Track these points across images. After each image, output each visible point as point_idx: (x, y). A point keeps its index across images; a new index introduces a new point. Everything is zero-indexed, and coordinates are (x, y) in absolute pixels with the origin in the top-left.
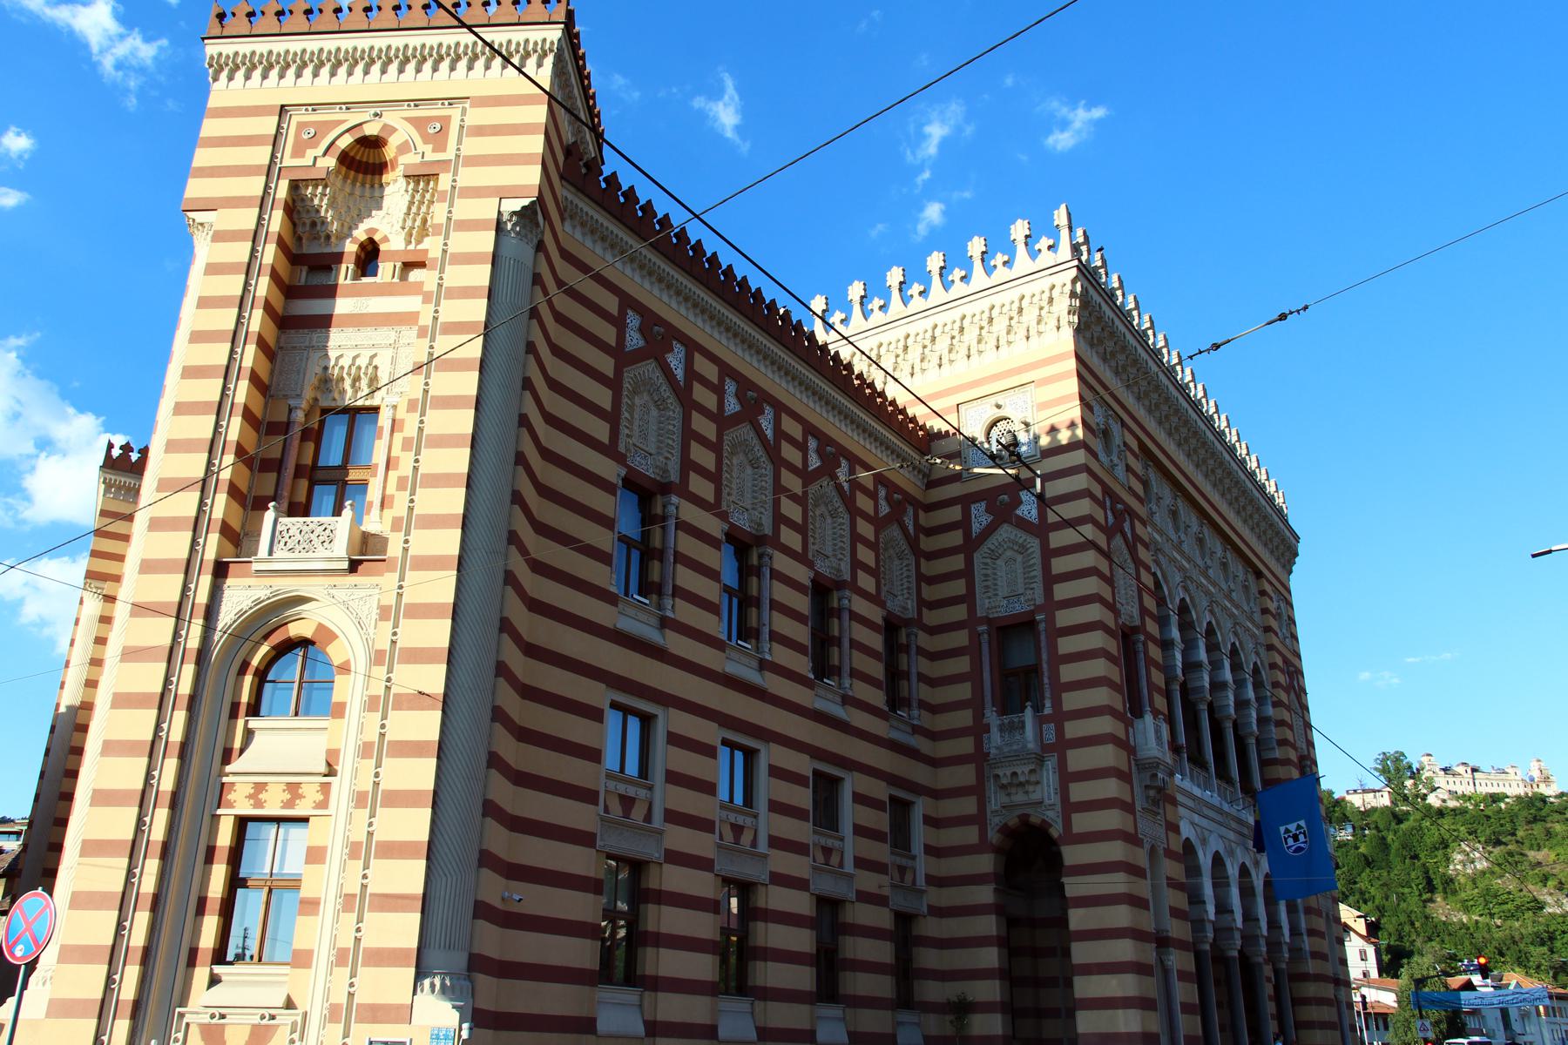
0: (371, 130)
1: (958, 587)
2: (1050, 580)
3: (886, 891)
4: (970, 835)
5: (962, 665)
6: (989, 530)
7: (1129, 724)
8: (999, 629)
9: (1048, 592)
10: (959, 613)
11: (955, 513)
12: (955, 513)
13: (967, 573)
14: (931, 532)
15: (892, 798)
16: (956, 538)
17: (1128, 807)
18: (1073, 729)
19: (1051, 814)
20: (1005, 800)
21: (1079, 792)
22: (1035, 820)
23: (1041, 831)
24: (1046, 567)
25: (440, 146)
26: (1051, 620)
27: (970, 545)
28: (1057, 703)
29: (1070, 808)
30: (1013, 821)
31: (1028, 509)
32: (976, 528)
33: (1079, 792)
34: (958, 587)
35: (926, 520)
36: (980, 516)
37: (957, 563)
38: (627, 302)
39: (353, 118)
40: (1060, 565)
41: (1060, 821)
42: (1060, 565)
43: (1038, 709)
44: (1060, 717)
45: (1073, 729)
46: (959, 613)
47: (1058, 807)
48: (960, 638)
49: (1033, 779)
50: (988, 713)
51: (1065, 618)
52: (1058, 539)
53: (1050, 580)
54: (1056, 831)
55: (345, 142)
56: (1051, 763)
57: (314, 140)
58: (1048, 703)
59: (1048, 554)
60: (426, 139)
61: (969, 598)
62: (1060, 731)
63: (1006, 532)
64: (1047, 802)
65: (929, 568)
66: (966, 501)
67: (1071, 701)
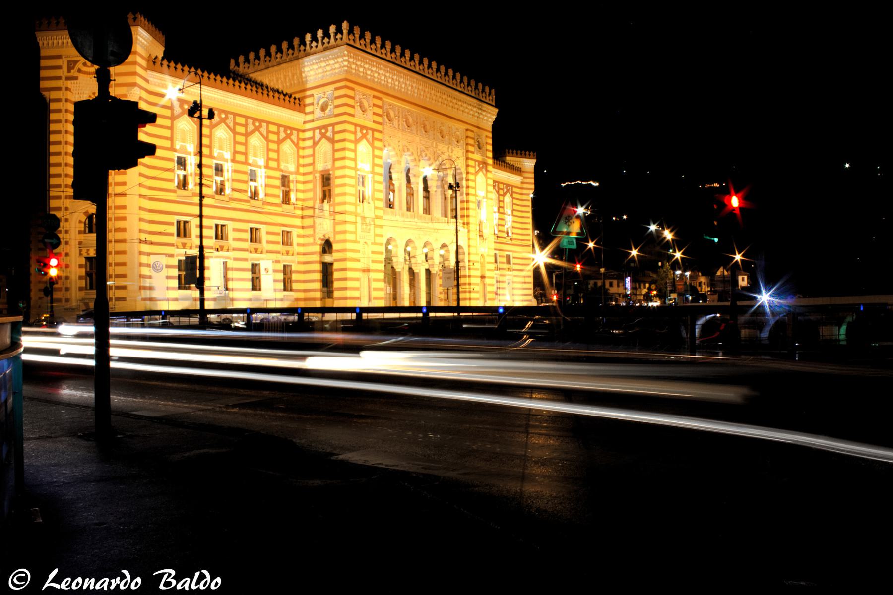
2: (334, 160)
4: (311, 240)
5: (310, 186)
6: (320, 140)
10: (309, 169)
11: (309, 134)
14: (304, 140)
27: (315, 144)
29: (336, 233)
31: (329, 134)
32: (316, 139)
35: (302, 135)
36: (318, 136)
37: (309, 152)
40: (338, 155)
44: (334, 205)
46: (309, 169)
48: (310, 177)
52: (338, 146)
53: (334, 160)
57: (73, 68)
59: (335, 151)
61: (313, 164)
63: (324, 140)
65: (301, 153)
66: (313, 130)
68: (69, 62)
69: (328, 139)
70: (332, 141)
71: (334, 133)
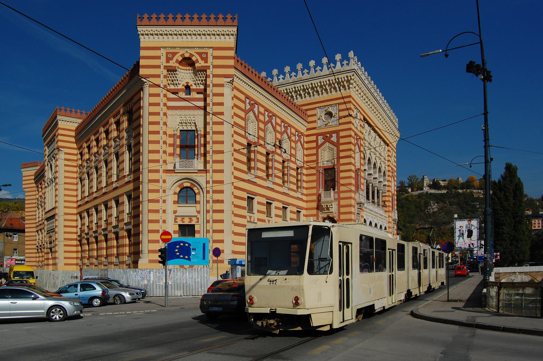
0: (187, 55)
1: (314, 158)
2: (339, 158)
5: (314, 178)
6: (323, 144)
8: (324, 169)
9: (338, 161)
11: (314, 138)
12: (314, 138)
13: (317, 154)
16: (314, 145)
21: (342, 210)
24: (338, 154)
25: (206, 62)
26: (339, 168)
27: (318, 147)
28: (339, 189)
31: (334, 138)
32: (320, 143)
33: (342, 210)
34: (314, 158)
36: (321, 140)
37: (314, 151)
38: (247, 97)
39: (182, 52)
40: (342, 154)
42: (342, 154)
43: (334, 190)
44: (339, 192)
45: (342, 195)
50: (321, 189)
51: (342, 168)
53: (339, 158)
55: (180, 59)
56: (336, 203)
57: (172, 59)
58: (336, 188)
59: (339, 151)
60: (202, 59)
61: (317, 161)
62: (339, 196)
66: (317, 135)
67: (342, 188)
68: (167, 53)
69: (332, 143)
70: (337, 144)
71: (338, 137)
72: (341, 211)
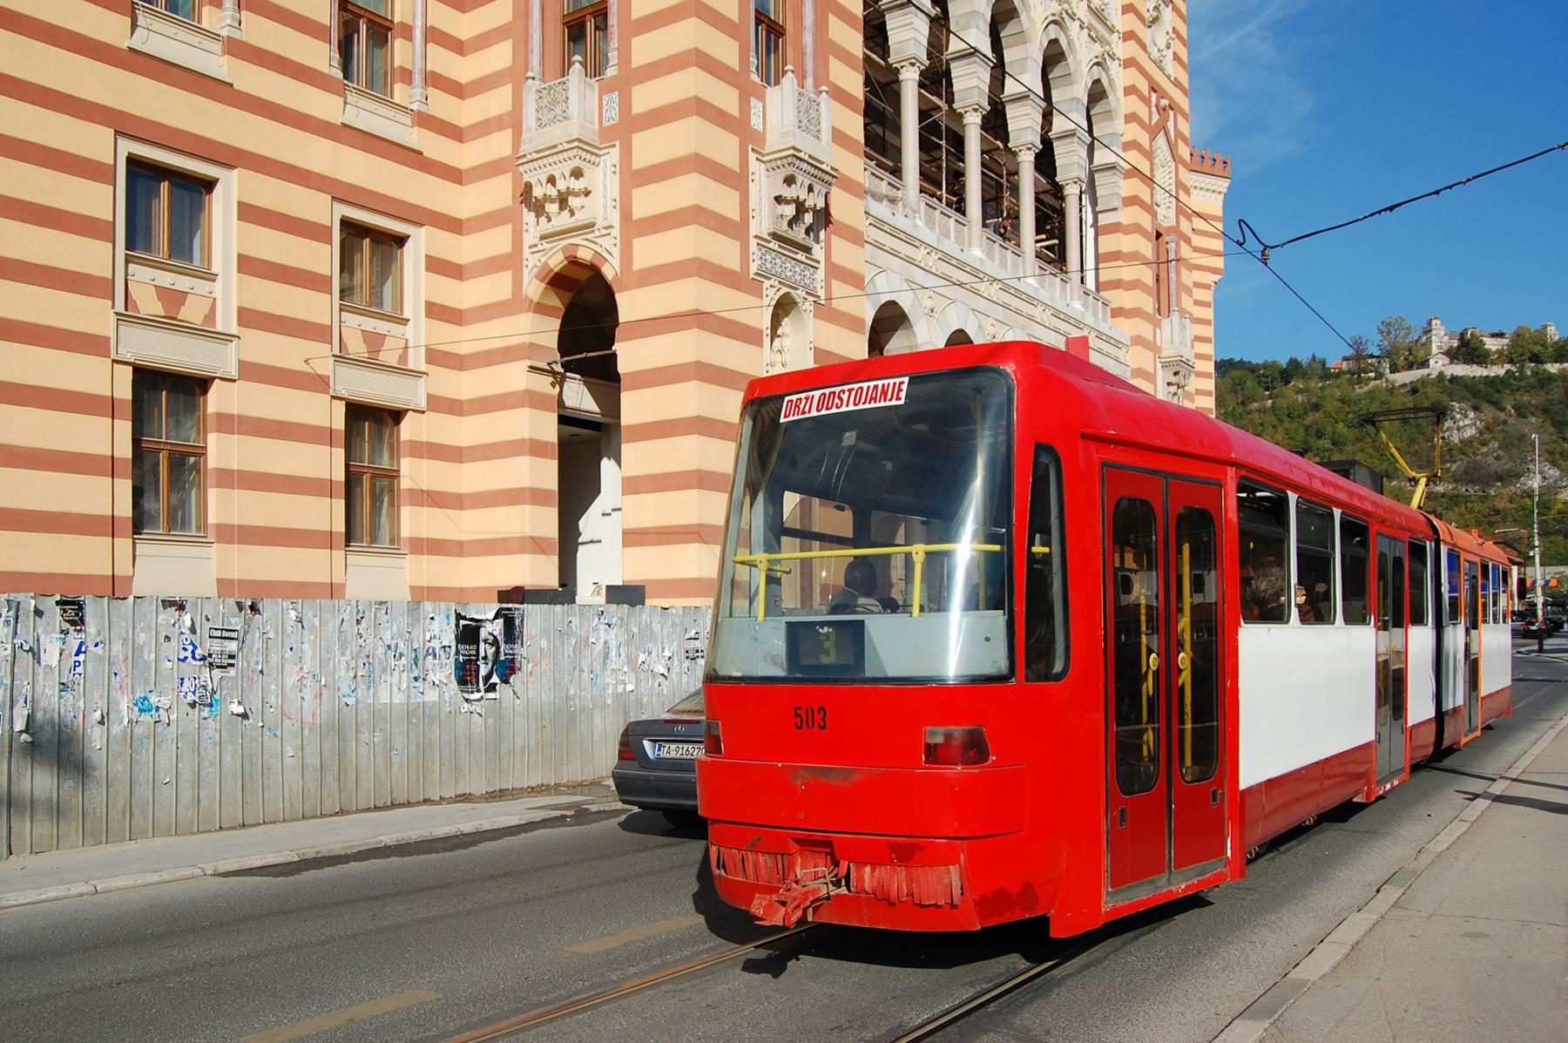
3: (325, 366)
7: (746, 94)
15: (346, 223)
17: (736, 229)
18: (646, 97)
19: (606, 243)
20: (545, 226)
22: (585, 255)
23: (594, 271)
30: (557, 262)
41: (616, 251)
43: (595, 69)
45: (646, 97)
47: (616, 232)
49: (577, 185)
54: (608, 272)
58: (613, 56)
62: (625, 104)
64: (600, 224)
67: (646, 48)
72: (638, 213)
